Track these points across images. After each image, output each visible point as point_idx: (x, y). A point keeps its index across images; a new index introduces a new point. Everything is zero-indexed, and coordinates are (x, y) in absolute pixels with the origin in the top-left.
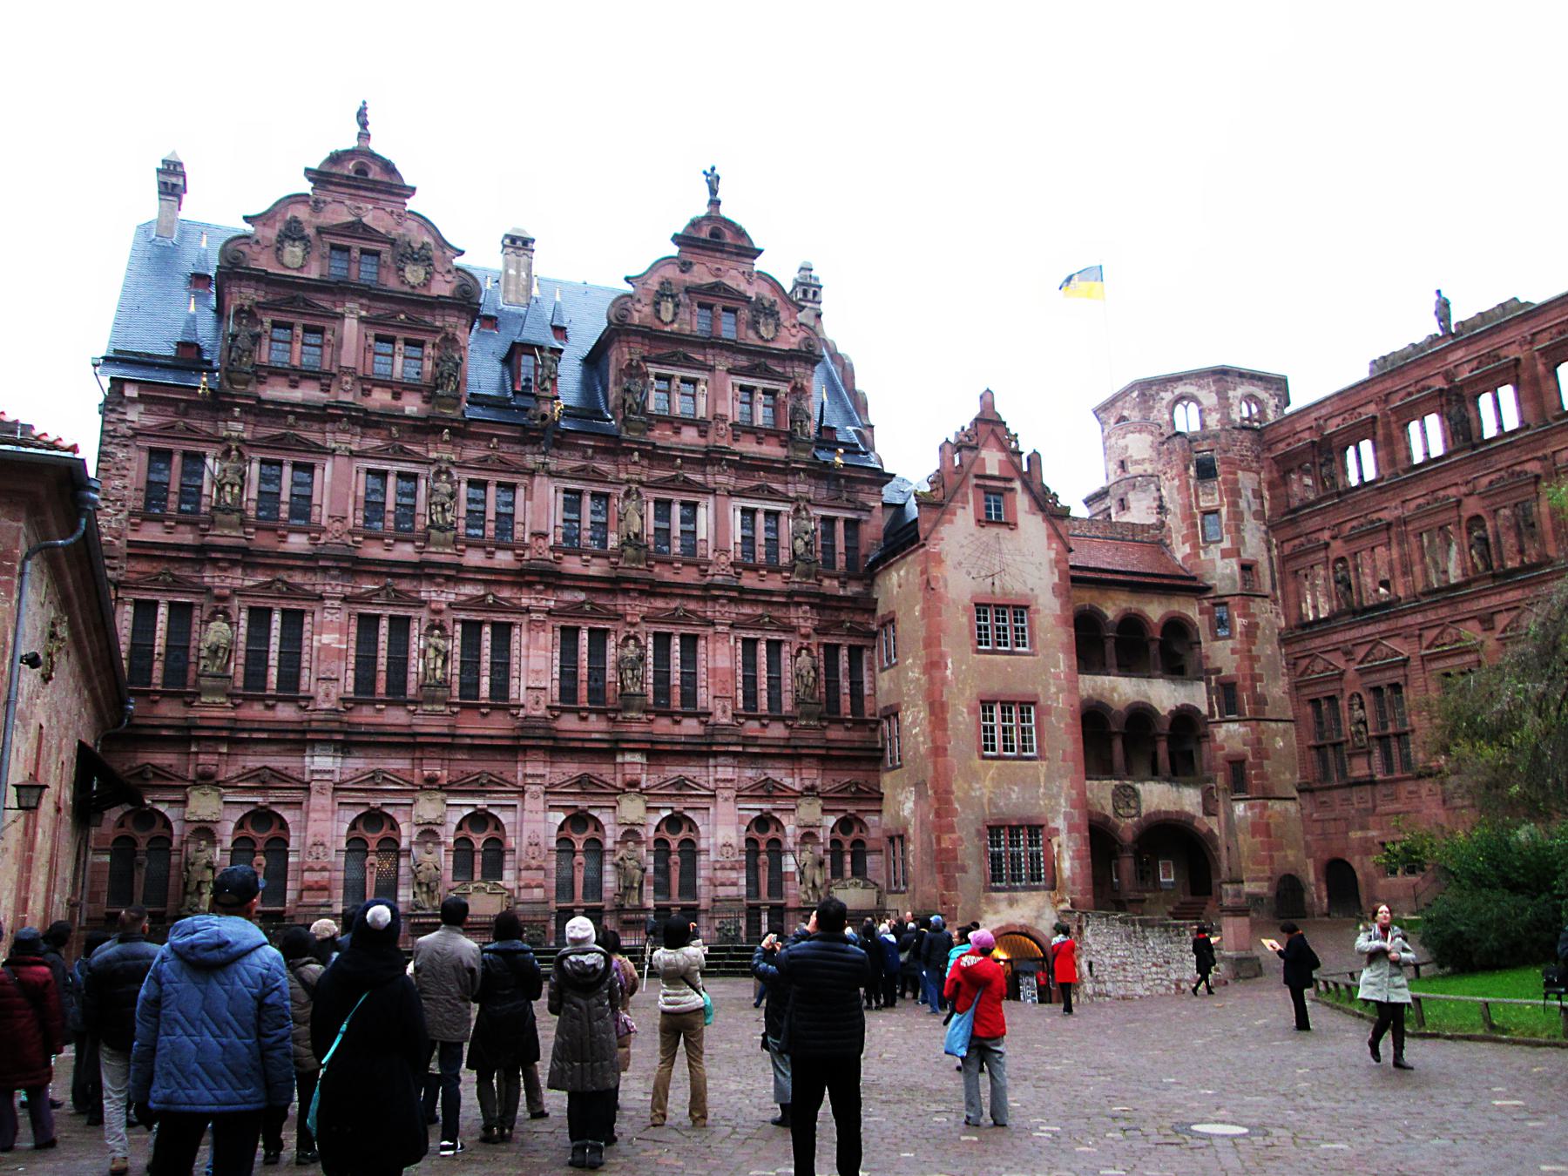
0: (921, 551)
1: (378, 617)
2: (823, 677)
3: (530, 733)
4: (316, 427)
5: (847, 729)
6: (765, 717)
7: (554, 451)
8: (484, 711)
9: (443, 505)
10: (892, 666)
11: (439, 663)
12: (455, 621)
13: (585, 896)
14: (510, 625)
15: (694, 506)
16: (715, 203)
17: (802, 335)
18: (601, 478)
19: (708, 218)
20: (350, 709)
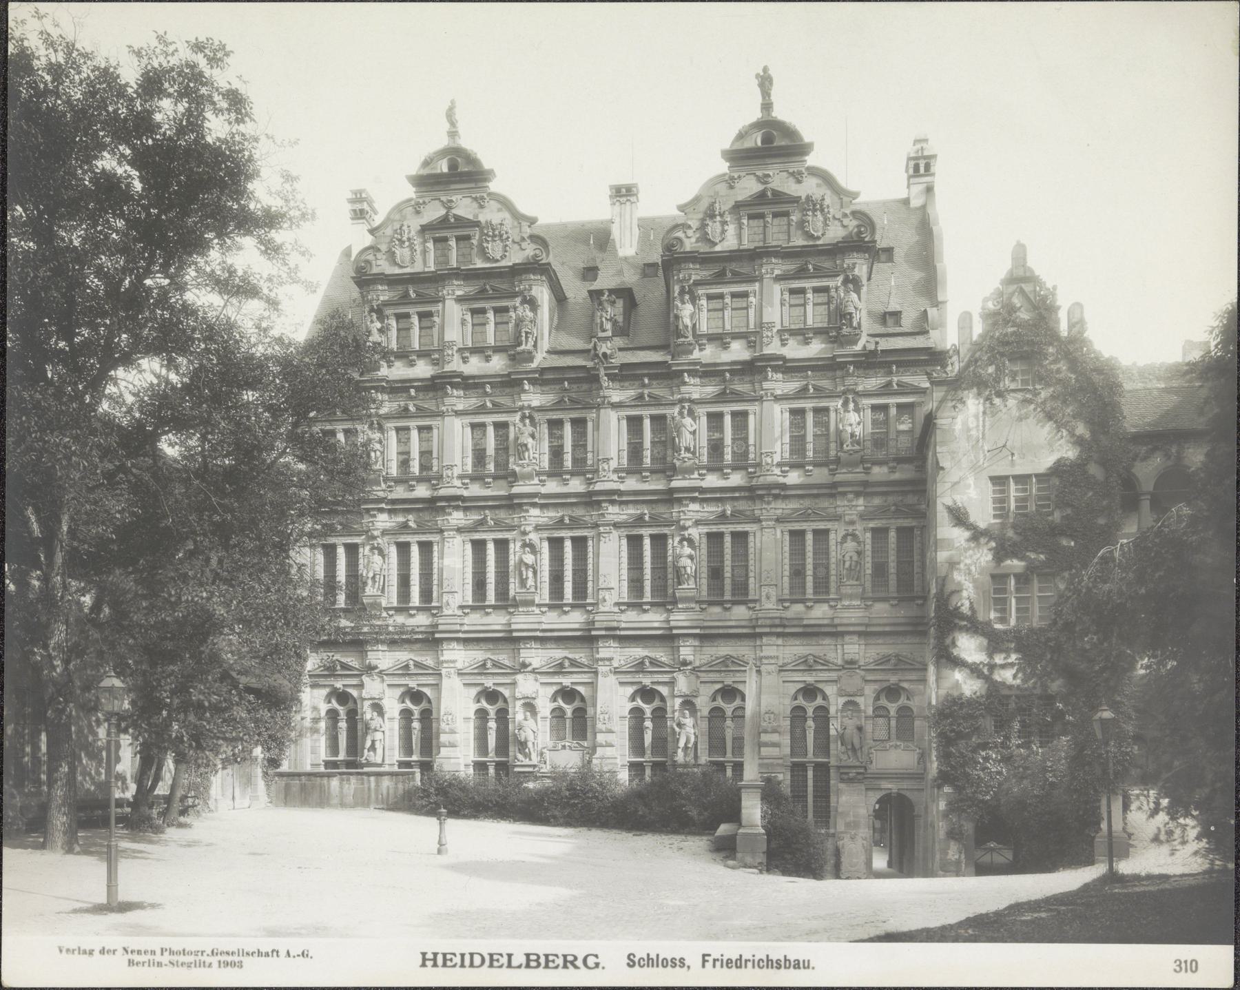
8: (566, 609)
11: (530, 574)
15: (745, 414)
16: (767, 106)
17: (852, 224)
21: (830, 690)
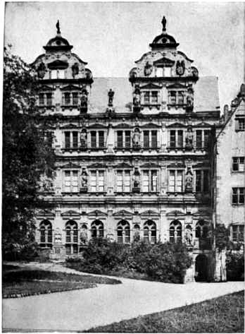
15: (156, 131)
17: (192, 70)
18: (127, 126)
19: (162, 36)
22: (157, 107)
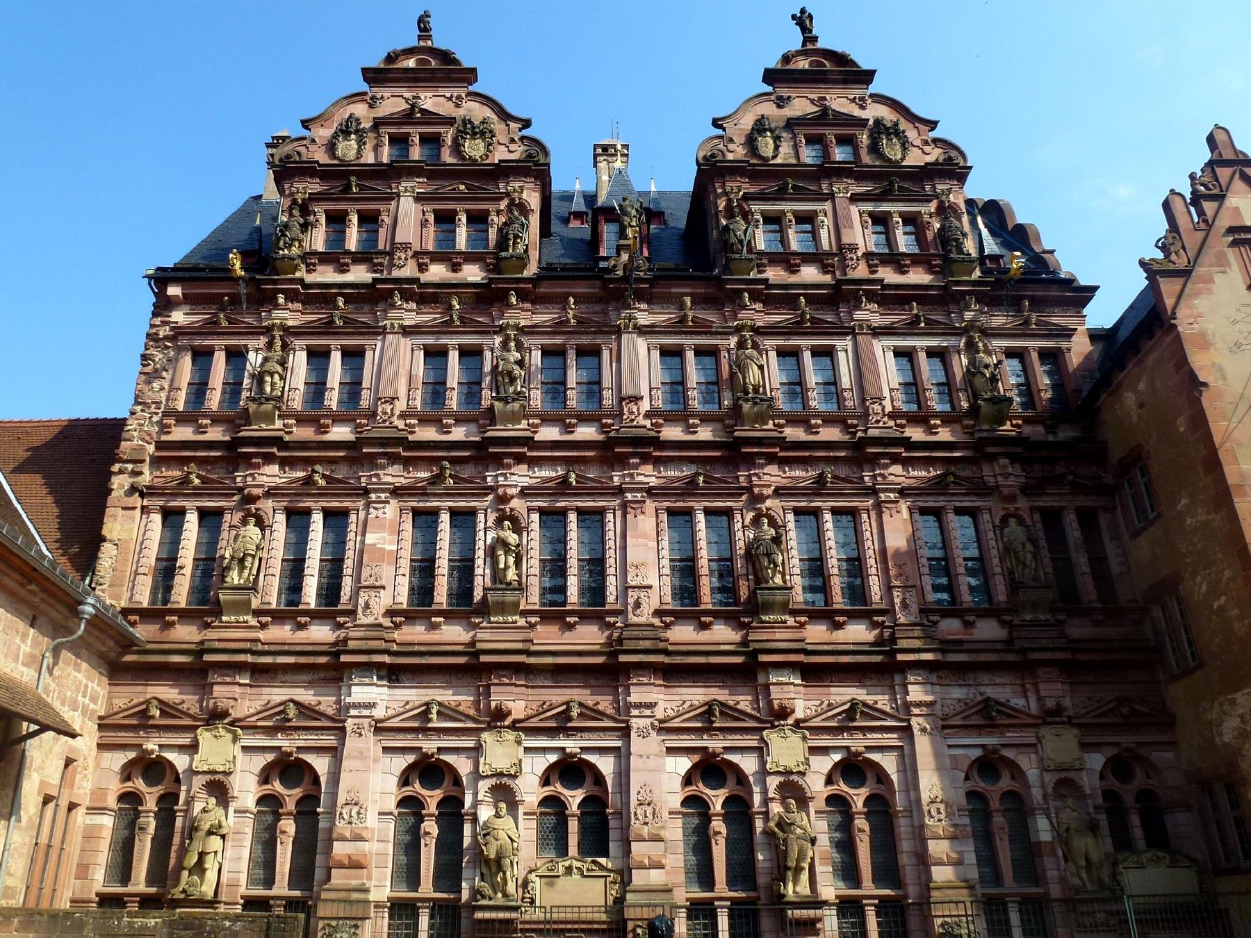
0: (1169, 339)
1: (435, 512)
2: (1045, 552)
3: (628, 645)
4: (367, 308)
5: (1097, 623)
6: (970, 610)
7: (643, 306)
9: (510, 374)
10: (1150, 523)
11: (511, 560)
12: (529, 510)
13: (731, 883)
14: (601, 512)
20: (397, 626)
21: (1028, 764)
22: (816, 258)
